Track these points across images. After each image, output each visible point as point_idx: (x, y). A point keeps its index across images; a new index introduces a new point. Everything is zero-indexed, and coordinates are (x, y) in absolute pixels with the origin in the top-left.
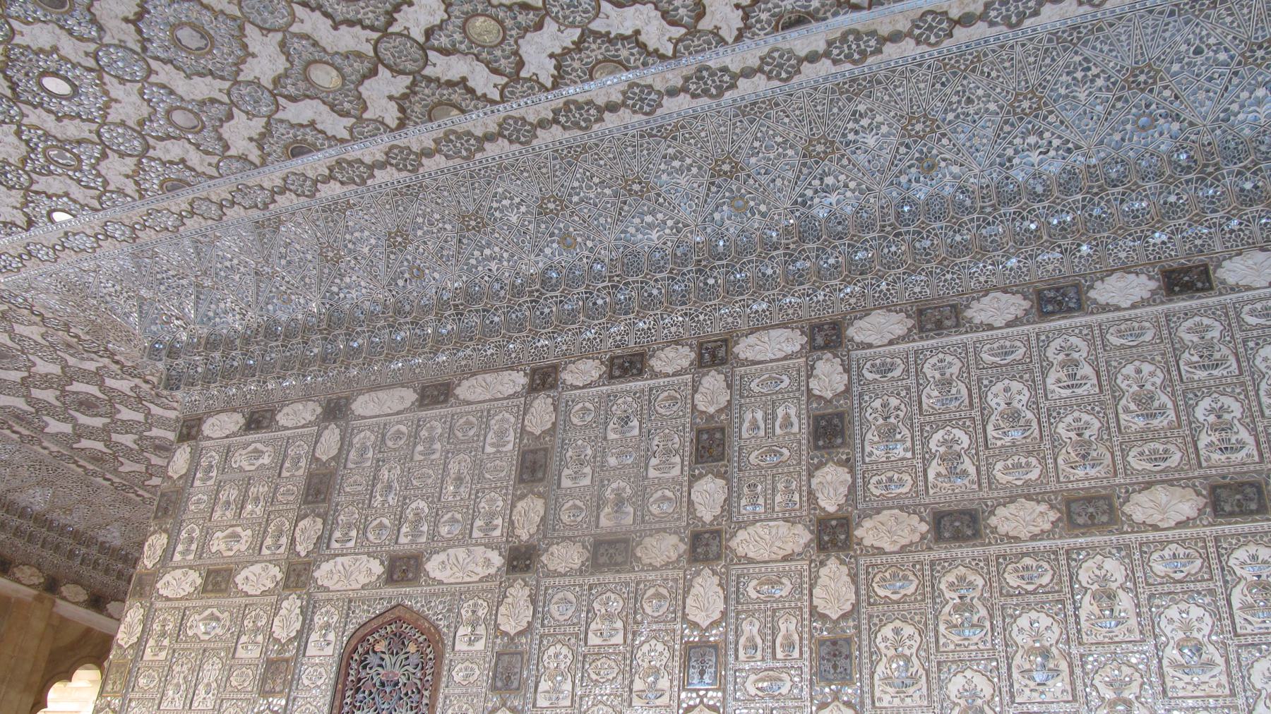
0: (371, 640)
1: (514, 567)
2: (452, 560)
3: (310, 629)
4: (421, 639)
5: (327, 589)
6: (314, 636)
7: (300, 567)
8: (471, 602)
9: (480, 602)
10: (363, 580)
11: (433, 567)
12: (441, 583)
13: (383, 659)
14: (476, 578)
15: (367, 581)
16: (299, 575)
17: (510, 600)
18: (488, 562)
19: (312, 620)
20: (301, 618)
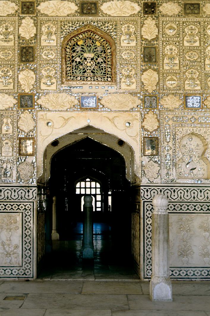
0: (75, 40)
1: (146, 11)
2: (114, 6)
3: (41, 34)
4: (102, 40)
5: (46, 15)
6: (44, 37)
7: (28, 4)
8: (126, 25)
9: (131, 25)
10: (67, 12)
11: (104, 8)
12: (109, 16)
13: (83, 48)
14: (128, 15)
15: (69, 12)
16: (28, 8)
17: (146, 25)
18: (133, 8)
19: (41, 29)
20: (35, 28)
